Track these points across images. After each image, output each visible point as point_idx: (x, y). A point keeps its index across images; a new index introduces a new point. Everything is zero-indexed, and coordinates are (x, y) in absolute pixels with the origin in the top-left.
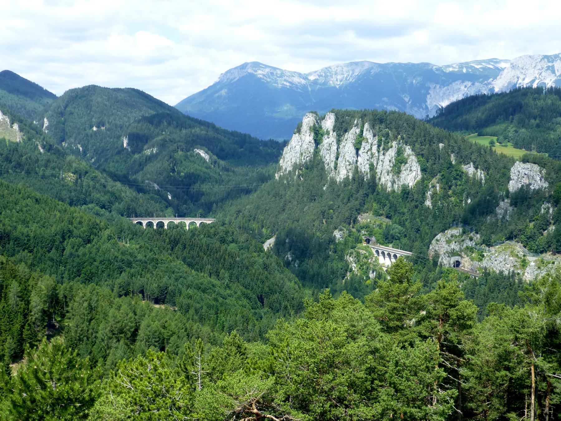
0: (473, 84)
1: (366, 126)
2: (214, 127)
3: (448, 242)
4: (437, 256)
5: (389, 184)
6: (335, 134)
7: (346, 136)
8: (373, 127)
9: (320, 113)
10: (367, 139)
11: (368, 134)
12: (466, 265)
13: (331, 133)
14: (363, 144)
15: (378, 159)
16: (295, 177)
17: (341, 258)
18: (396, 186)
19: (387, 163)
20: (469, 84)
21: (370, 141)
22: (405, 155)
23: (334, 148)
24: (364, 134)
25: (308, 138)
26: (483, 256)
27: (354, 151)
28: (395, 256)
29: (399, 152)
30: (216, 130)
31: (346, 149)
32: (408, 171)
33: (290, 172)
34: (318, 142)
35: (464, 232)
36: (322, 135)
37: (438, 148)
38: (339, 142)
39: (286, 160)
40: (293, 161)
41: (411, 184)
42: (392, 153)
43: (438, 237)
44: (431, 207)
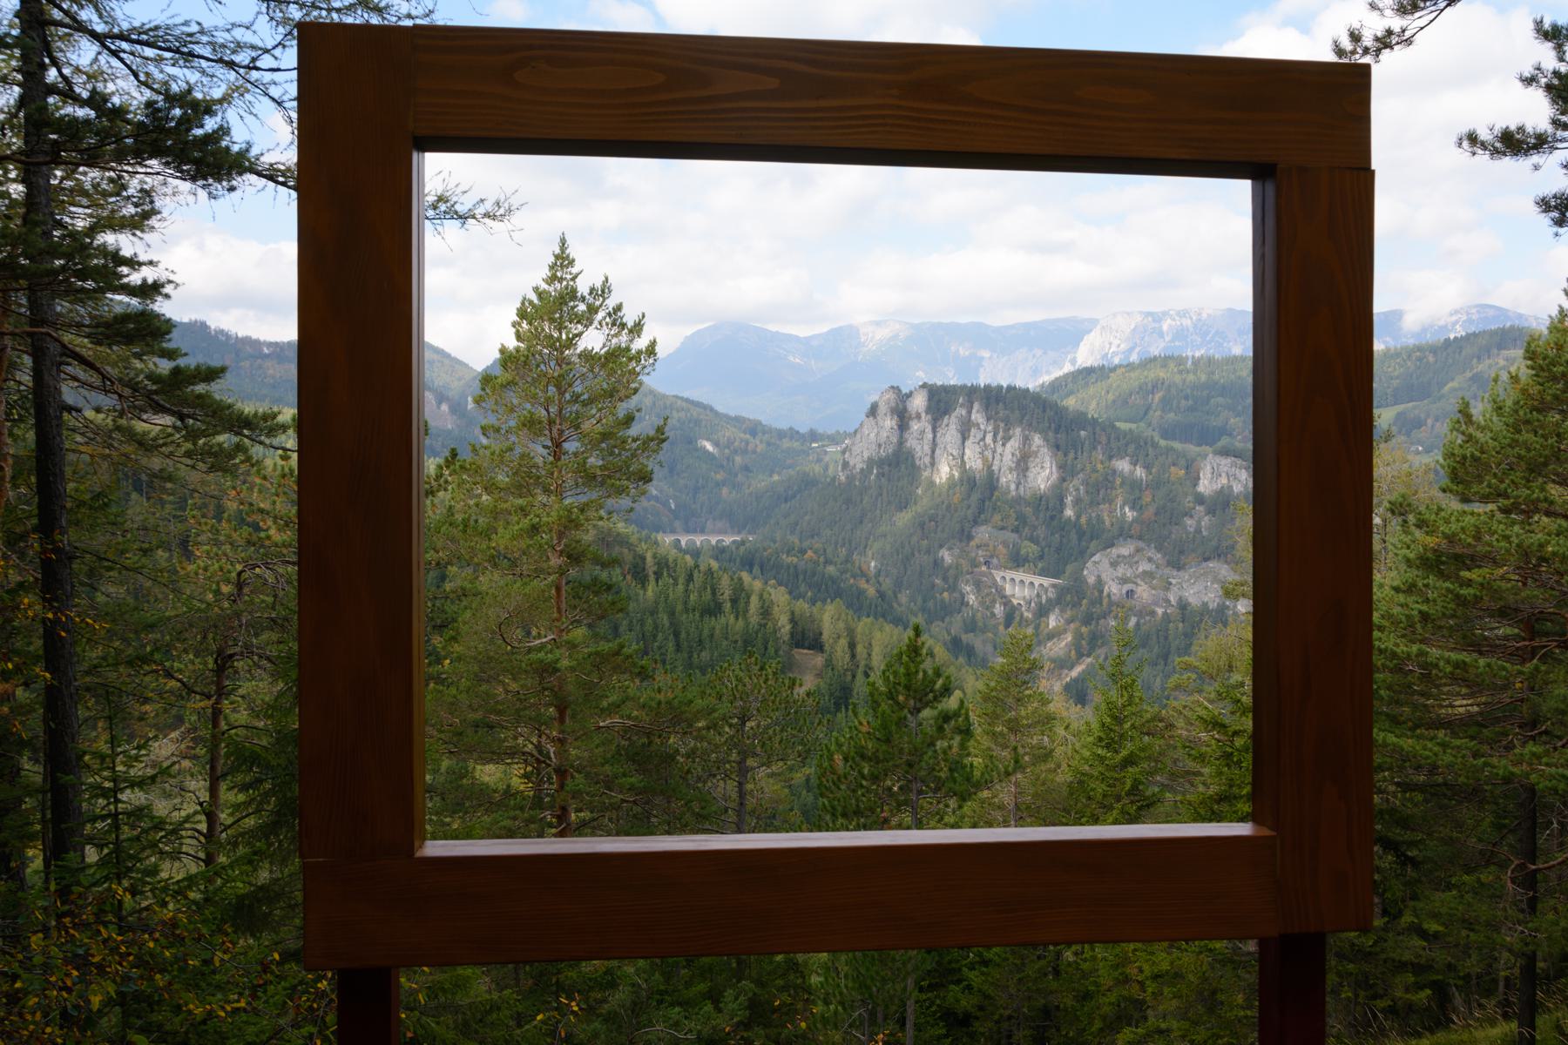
0: (1045, 353)
1: (976, 406)
2: (712, 409)
3: (1114, 565)
4: (1100, 583)
5: (1013, 487)
6: (929, 417)
7: (946, 421)
8: (986, 407)
9: (905, 390)
10: (978, 425)
11: (977, 416)
12: (1145, 595)
13: (923, 415)
14: (973, 431)
15: (994, 452)
16: (873, 477)
17: (953, 588)
18: (1022, 489)
19: (1008, 458)
20: (1039, 352)
21: (982, 427)
22: (1034, 448)
23: (930, 436)
24: (973, 417)
25: (889, 423)
26: (1170, 584)
27: (959, 442)
28: (1032, 583)
29: (1026, 440)
30: (716, 413)
31: (948, 438)
32: (1038, 469)
33: (862, 470)
34: (903, 426)
35: (1138, 550)
36: (910, 418)
37: (1079, 436)
38: (934, 431)
39: (854, 453)
40: (866, 455)
41: (1042, 487)
42: (1013, 445)
43: (1096, 558)
44: (1073, 518)
